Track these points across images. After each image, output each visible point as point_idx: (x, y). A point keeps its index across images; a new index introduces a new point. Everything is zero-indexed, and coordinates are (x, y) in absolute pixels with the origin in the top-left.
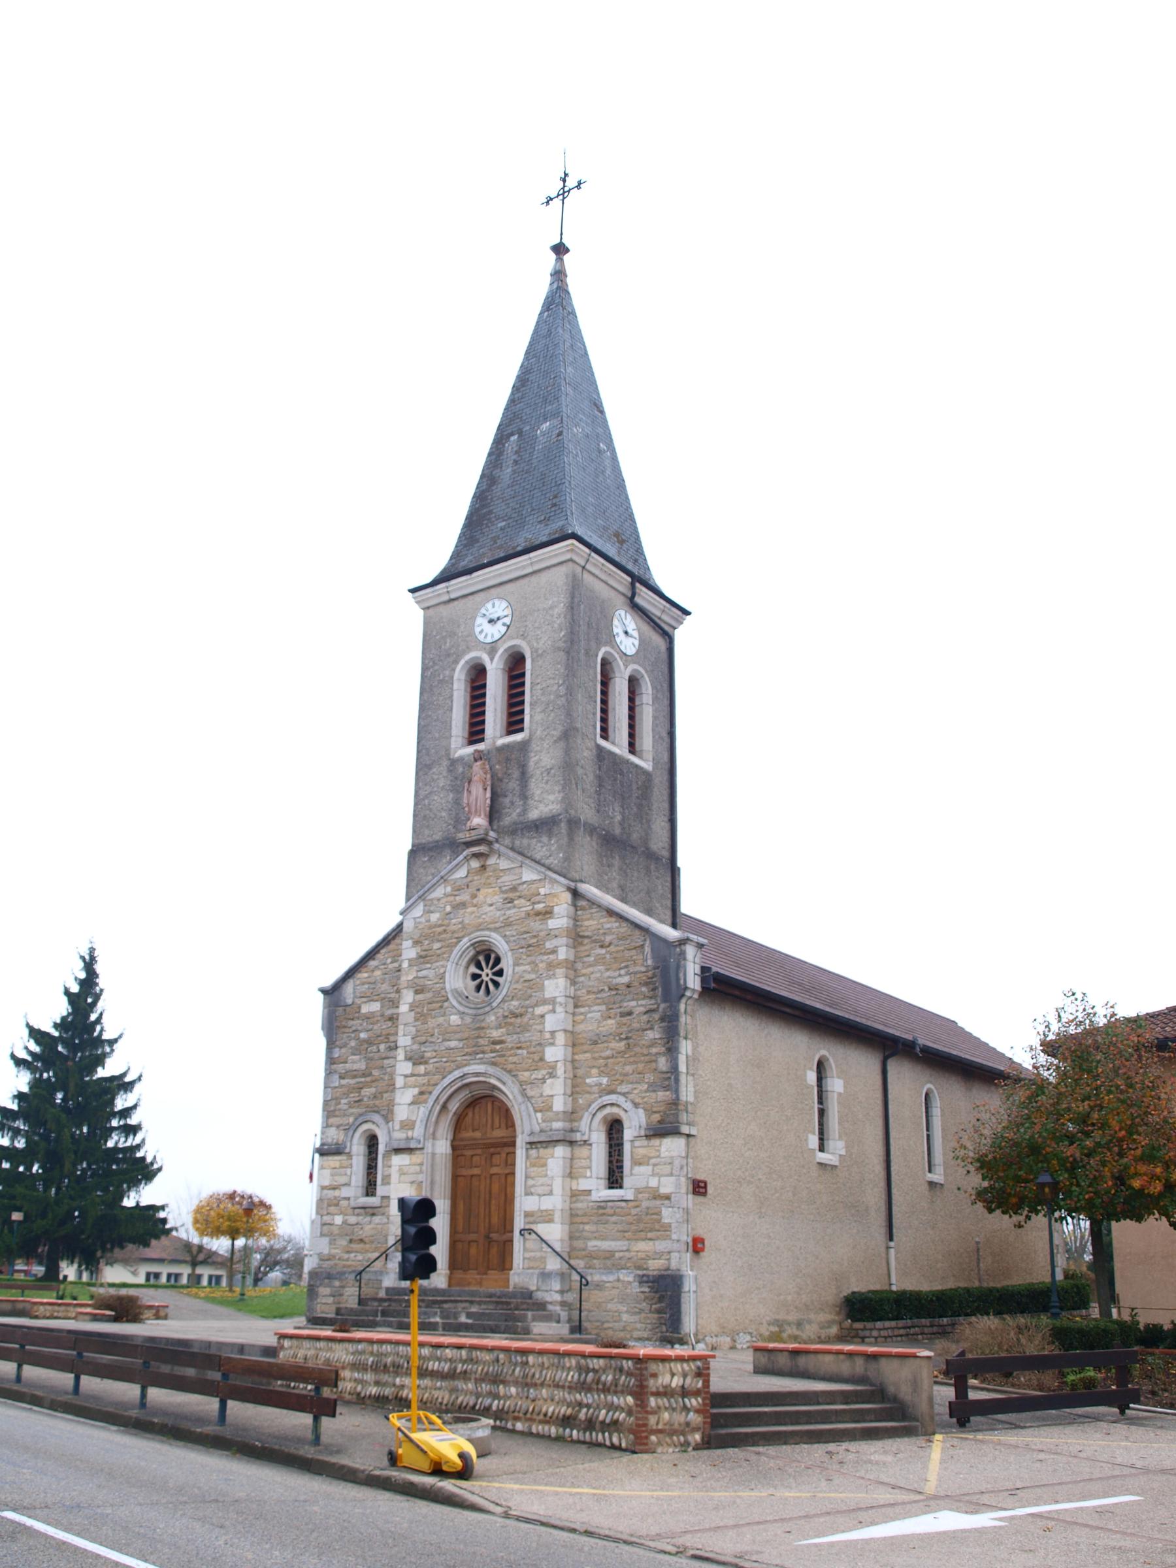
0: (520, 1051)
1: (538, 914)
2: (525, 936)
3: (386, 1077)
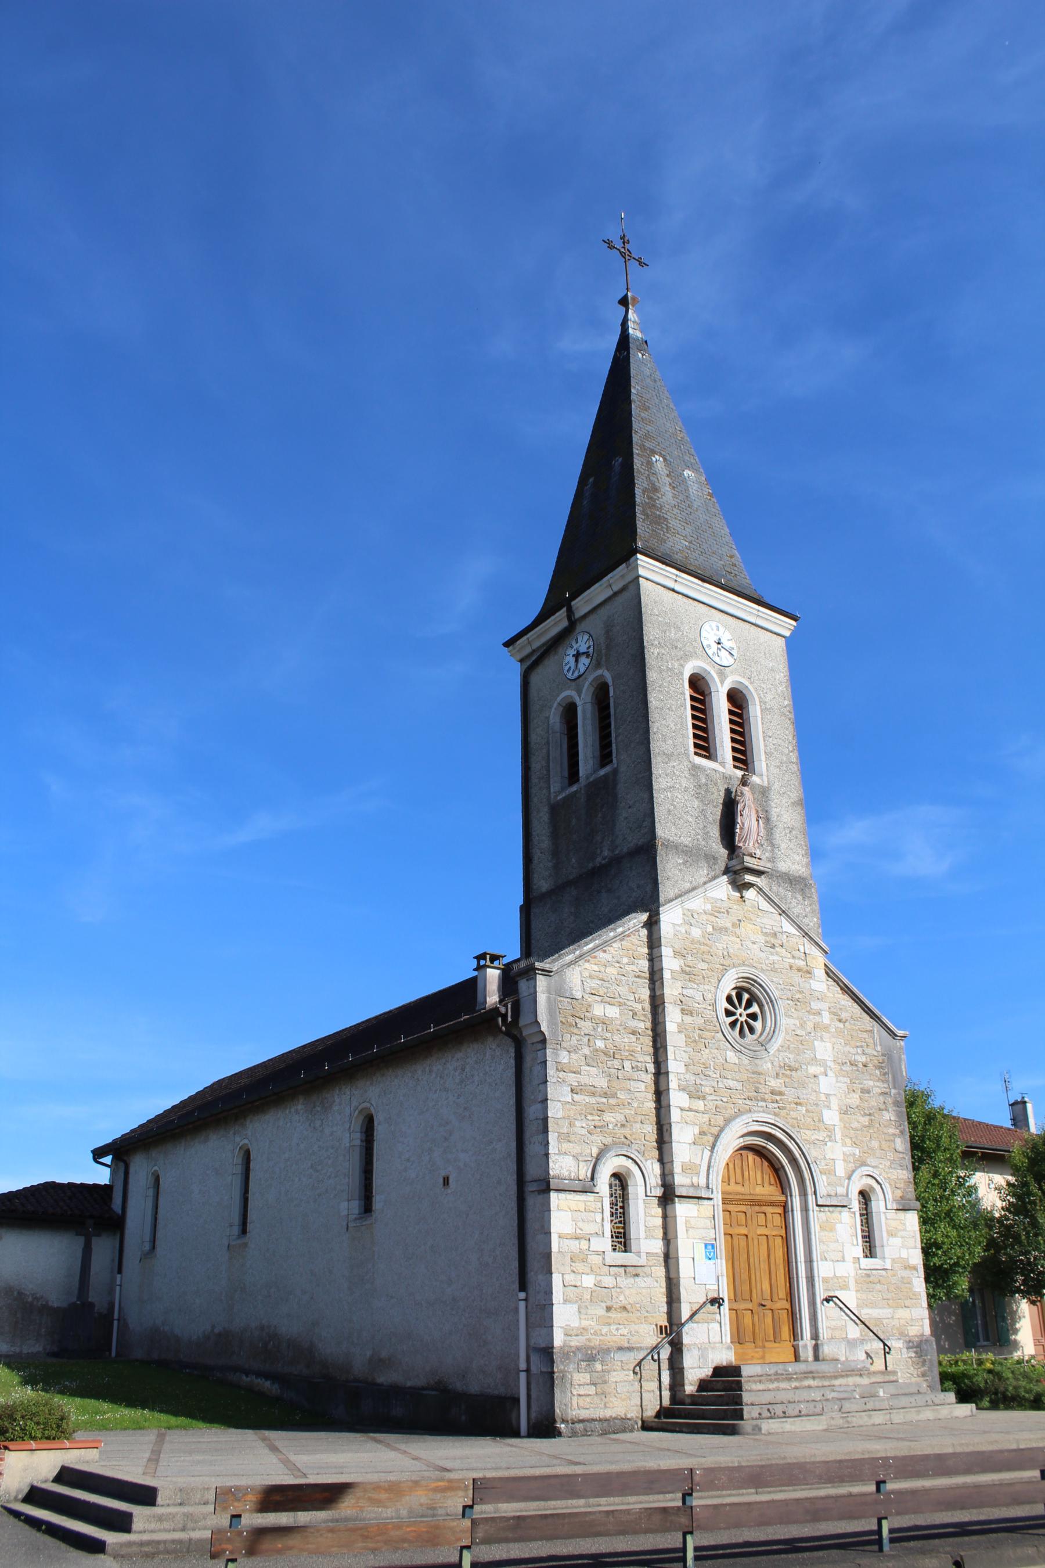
0: (799, 1107)
1: (799, 970)
2: (791, 988)
3: (635, 1105)
